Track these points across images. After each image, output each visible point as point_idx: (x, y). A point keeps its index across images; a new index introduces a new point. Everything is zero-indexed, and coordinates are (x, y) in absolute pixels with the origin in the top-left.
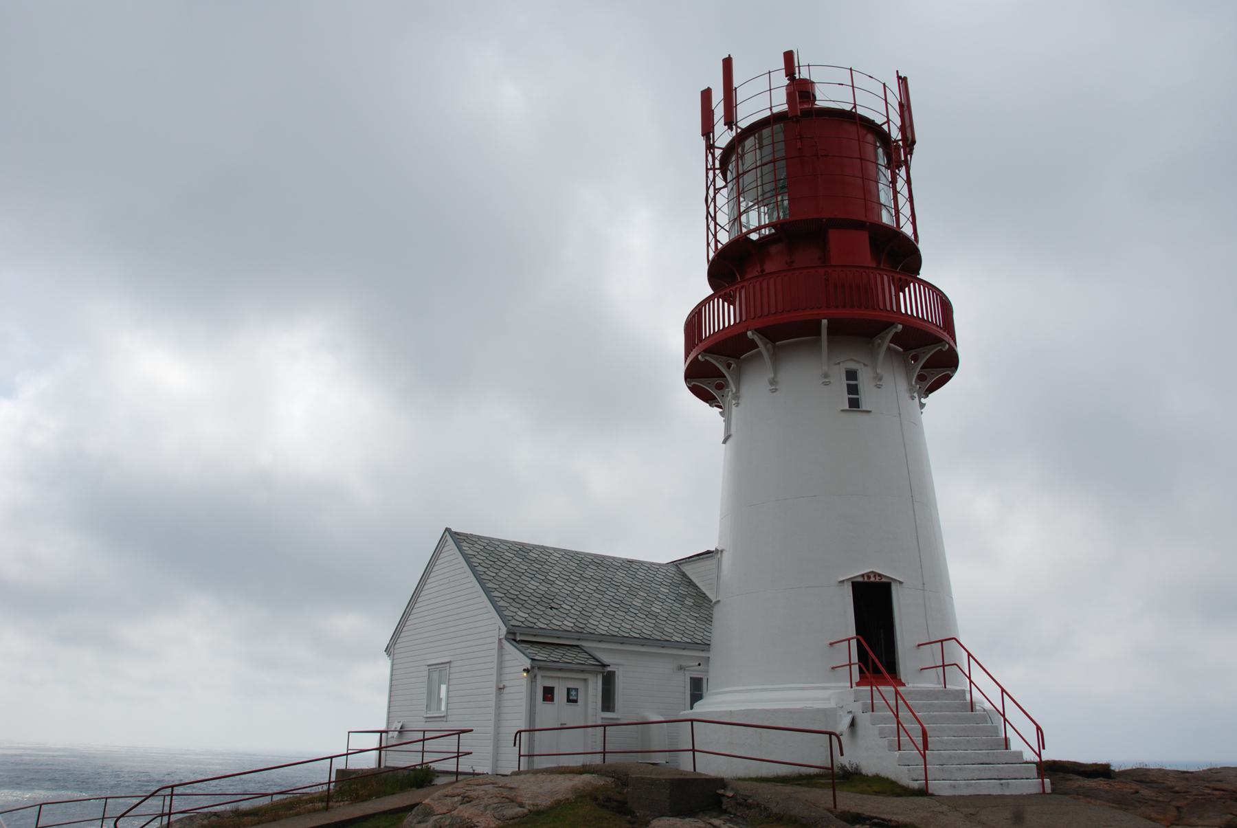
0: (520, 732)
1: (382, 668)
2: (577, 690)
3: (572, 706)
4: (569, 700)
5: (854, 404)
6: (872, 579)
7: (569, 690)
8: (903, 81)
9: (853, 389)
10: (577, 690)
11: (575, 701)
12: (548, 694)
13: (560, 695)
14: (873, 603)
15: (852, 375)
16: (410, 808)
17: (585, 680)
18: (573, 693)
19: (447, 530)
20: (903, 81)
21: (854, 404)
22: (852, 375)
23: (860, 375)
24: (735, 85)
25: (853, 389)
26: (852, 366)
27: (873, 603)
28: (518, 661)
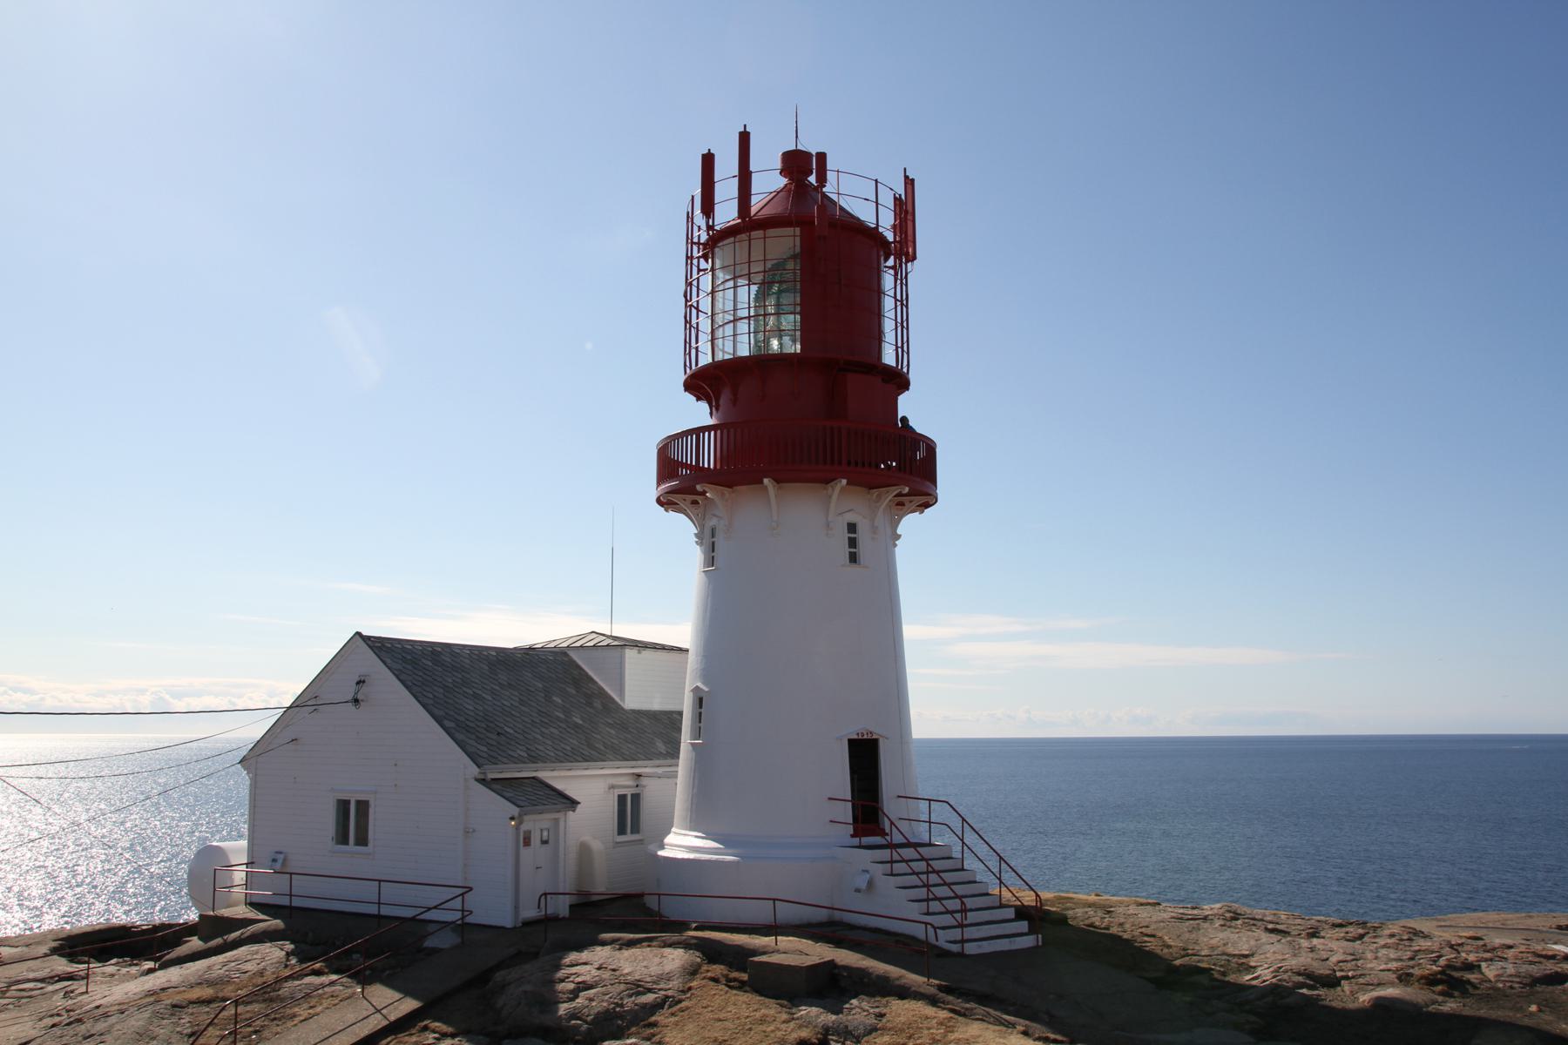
5: (853, 558)
8: (909, 183)
9: (853, 543)
15: (852, 528)
20: (909, 183)
21: (853, 558)
22: (852, 528)
23: (859, 528)
25: (853, 543)
26: (851, 517)
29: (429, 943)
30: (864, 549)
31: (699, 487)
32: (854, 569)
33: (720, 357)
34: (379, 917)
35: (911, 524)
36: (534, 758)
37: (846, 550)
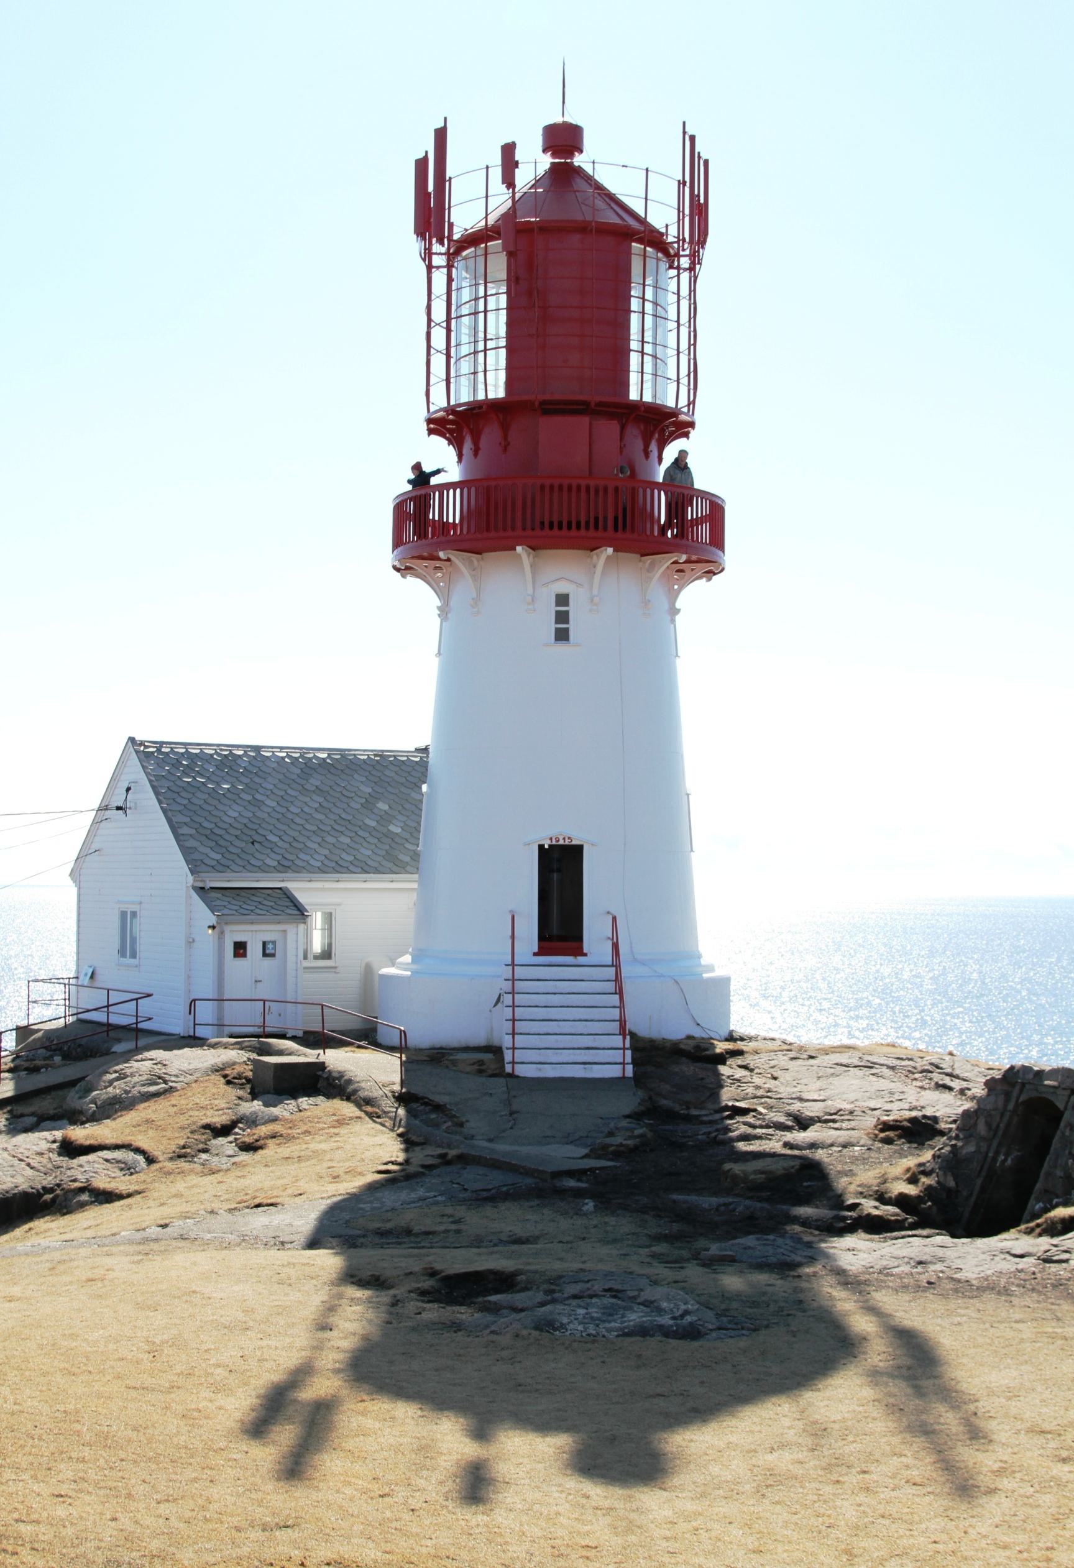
0: (194, 1000)
1: (70, 893)
2: (274, 943)
3: (268, 961)
4: (265, 955)
5: (562, 636)
6: (561, 842)
7: (264, 944)
9: (562, 617)
10: (274, 943)
11: (273, 955)
12: (240, 949)
13: (254, 950)
14: (560, 868)
15: (562, 599)
16: (73, 1083)
17: (285, 931)
18: (270, 946)
19: (132, 740)
21: (562, 636)
22: (562, 599)
24: (449, 173)
25: (562, 617)
26: (562, 588)
27: (560, 868)
28: (204, 916)
29: (114, 1049)
30: (574, 626)
31: (442, 554)
32: (562, 647)
33: (491, 396)
34: (108, 1025)
35: (696, 597)
36: (284, 867)
37: (551, 626)
